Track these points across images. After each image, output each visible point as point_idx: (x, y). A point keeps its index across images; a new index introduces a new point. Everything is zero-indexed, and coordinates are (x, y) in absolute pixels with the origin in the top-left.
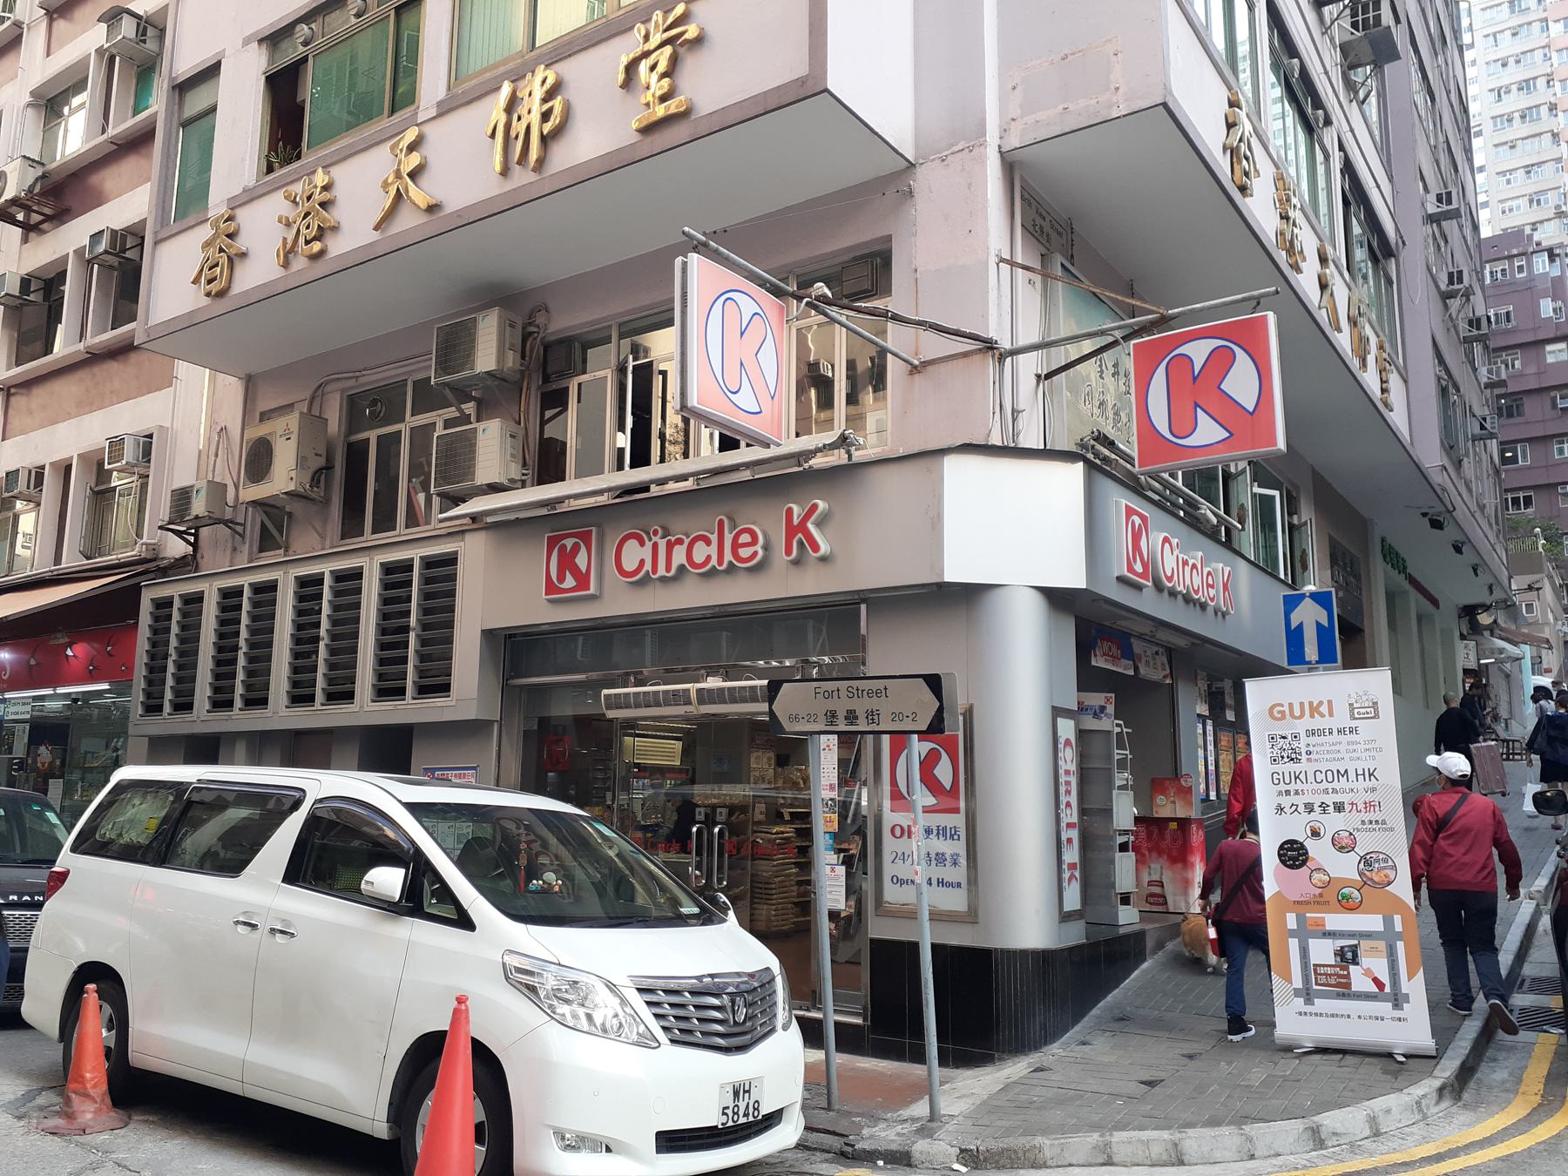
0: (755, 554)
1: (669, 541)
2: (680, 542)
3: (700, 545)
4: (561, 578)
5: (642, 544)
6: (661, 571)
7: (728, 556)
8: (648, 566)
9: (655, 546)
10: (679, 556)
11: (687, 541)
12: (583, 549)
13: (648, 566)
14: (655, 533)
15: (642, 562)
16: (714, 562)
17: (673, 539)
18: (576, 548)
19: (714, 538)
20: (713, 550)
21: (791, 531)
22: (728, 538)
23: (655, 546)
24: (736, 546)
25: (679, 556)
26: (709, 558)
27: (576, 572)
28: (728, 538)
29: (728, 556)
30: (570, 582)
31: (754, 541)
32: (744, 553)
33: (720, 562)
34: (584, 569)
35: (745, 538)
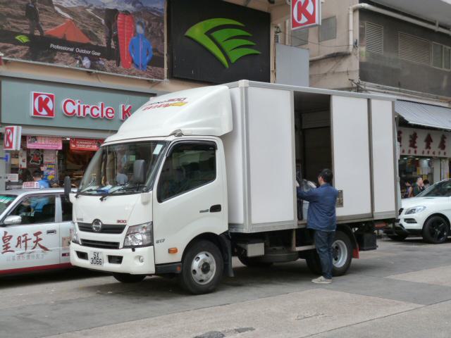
2: (88, 107)
3: (95, 109)
4: (41, 110)
6: (82, 114)
7: (104, 114)
8: (77, 112)
9: (79, 106)
10: (88, 111)
11: (91, 107)
12: (50, 101)
13: (77, 112)
15: (74, 111)
16: (100, 115)
18: (47, 100)
19: (100, 107)
20: (100, 112)
22: (105, 110)
23: (79, 106)
24: (107, 112)
25: (88, 111)
26: (98, 114)
27: (47, 109)
28: (105, 110)
29: (104, 114)
30: (44, 112)
32: (110, 115)
33: (102, 114)
34: (51, 109)
35: (110, 111)
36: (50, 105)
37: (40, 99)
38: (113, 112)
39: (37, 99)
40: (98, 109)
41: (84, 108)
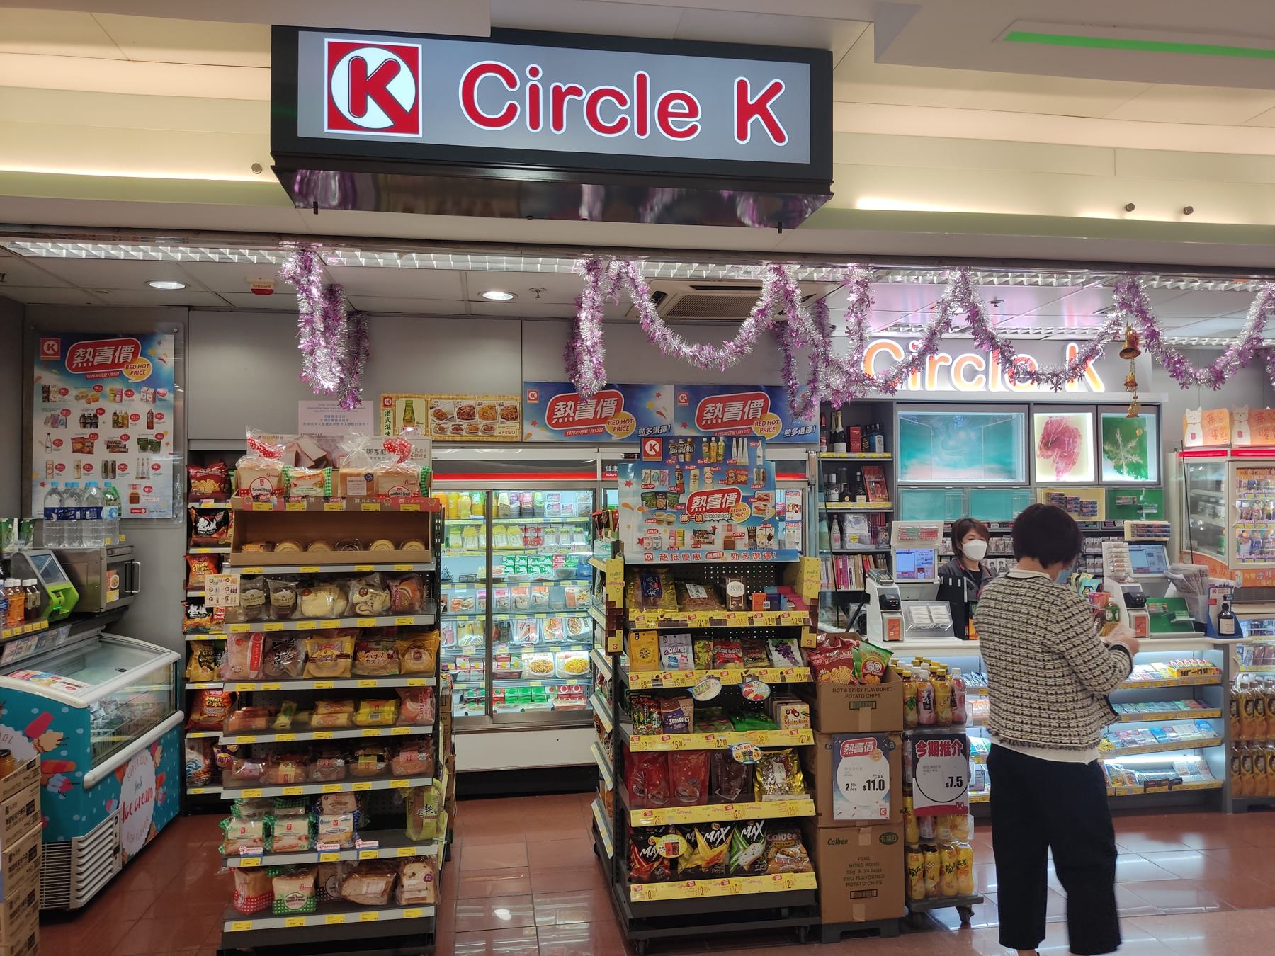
0: (694, 128)
1: (557, 89)
2: (578, 92)
4: (358, 107)
5: (512, 82)
9: (534, 89)
11: (586, 97)
14: (534, 72)
15: (512, 110)
17: (564, 88)
21: (745, 111)
23: (534, 89)
24: (664, 114)
26: (623, 122)
30: (375, 118)
31: (693, 112)
34: (407, 105)
36: (402, 88)
37: (358, 66)
38: (693, 112)
39: (343, 68)
40: (622, 101)
41: (559, 95)
